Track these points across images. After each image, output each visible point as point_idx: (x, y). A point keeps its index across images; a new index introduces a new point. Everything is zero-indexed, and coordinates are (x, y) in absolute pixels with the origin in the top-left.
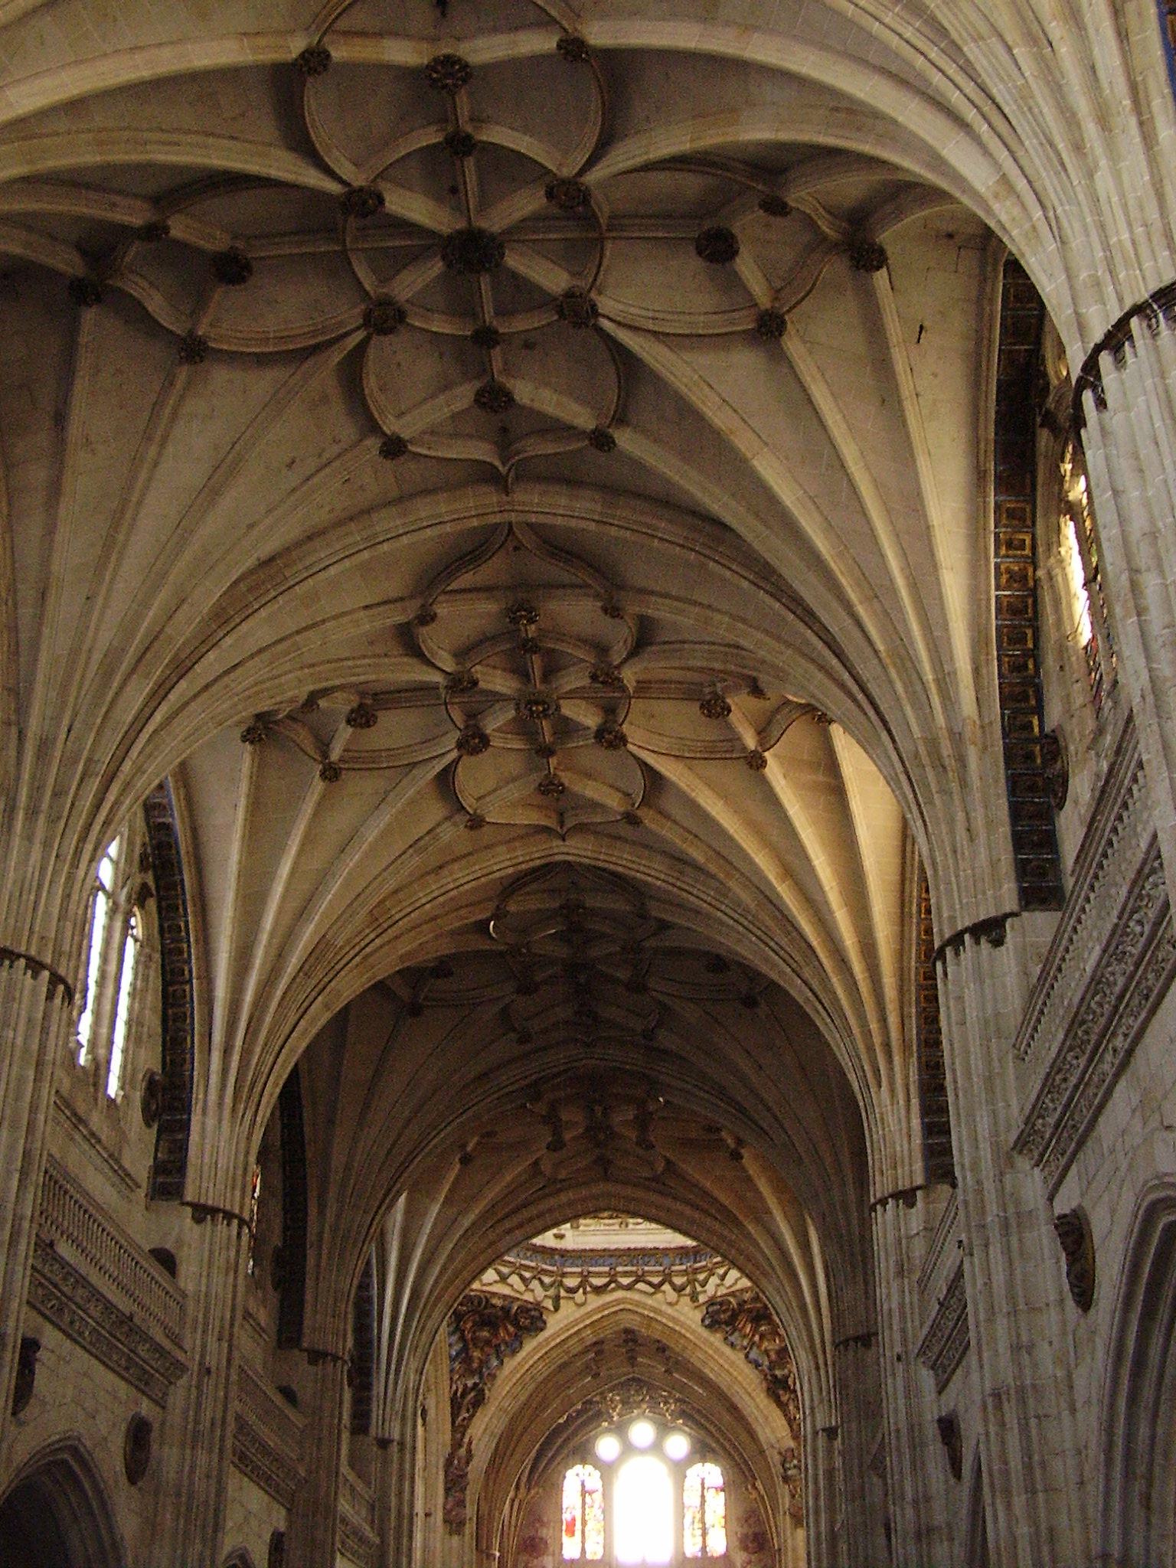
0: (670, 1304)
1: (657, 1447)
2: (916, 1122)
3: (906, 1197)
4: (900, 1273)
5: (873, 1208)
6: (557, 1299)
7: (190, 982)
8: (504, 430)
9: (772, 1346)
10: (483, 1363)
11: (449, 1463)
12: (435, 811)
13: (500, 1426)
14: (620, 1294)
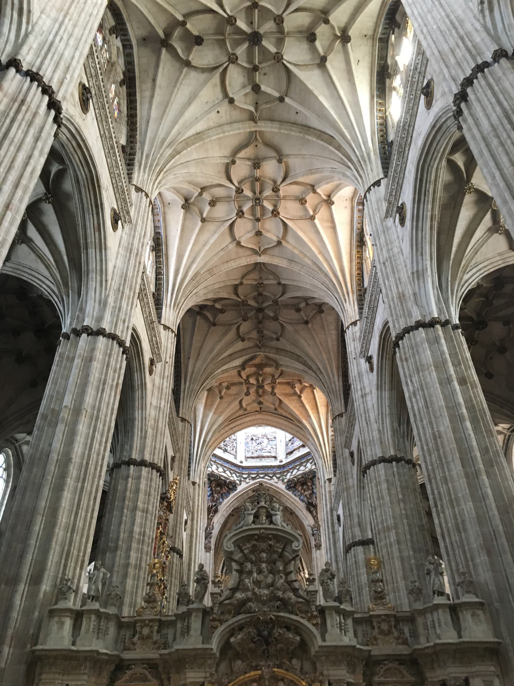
2: (356, 307)
3: (354, 323)
4: (354, 340)
5: (345, 332)
6: (241, 481)
8: (257, 103)
9: (306, 493)
11: (206, 529)
12: (228, 239)
13: (222, 521)
14: (260, 480)
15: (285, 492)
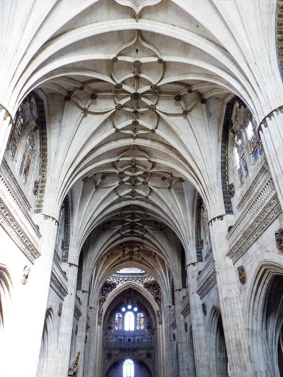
0: (138, 283)
1: (132, 310)
2: (195, 251)
3: (194, 264)
4: (193, 277)
5: (187, 266)
7: (70, 223)
10: (106, 294)
11: (99, 312)
14: (129, 281)
15: (143, 289)
